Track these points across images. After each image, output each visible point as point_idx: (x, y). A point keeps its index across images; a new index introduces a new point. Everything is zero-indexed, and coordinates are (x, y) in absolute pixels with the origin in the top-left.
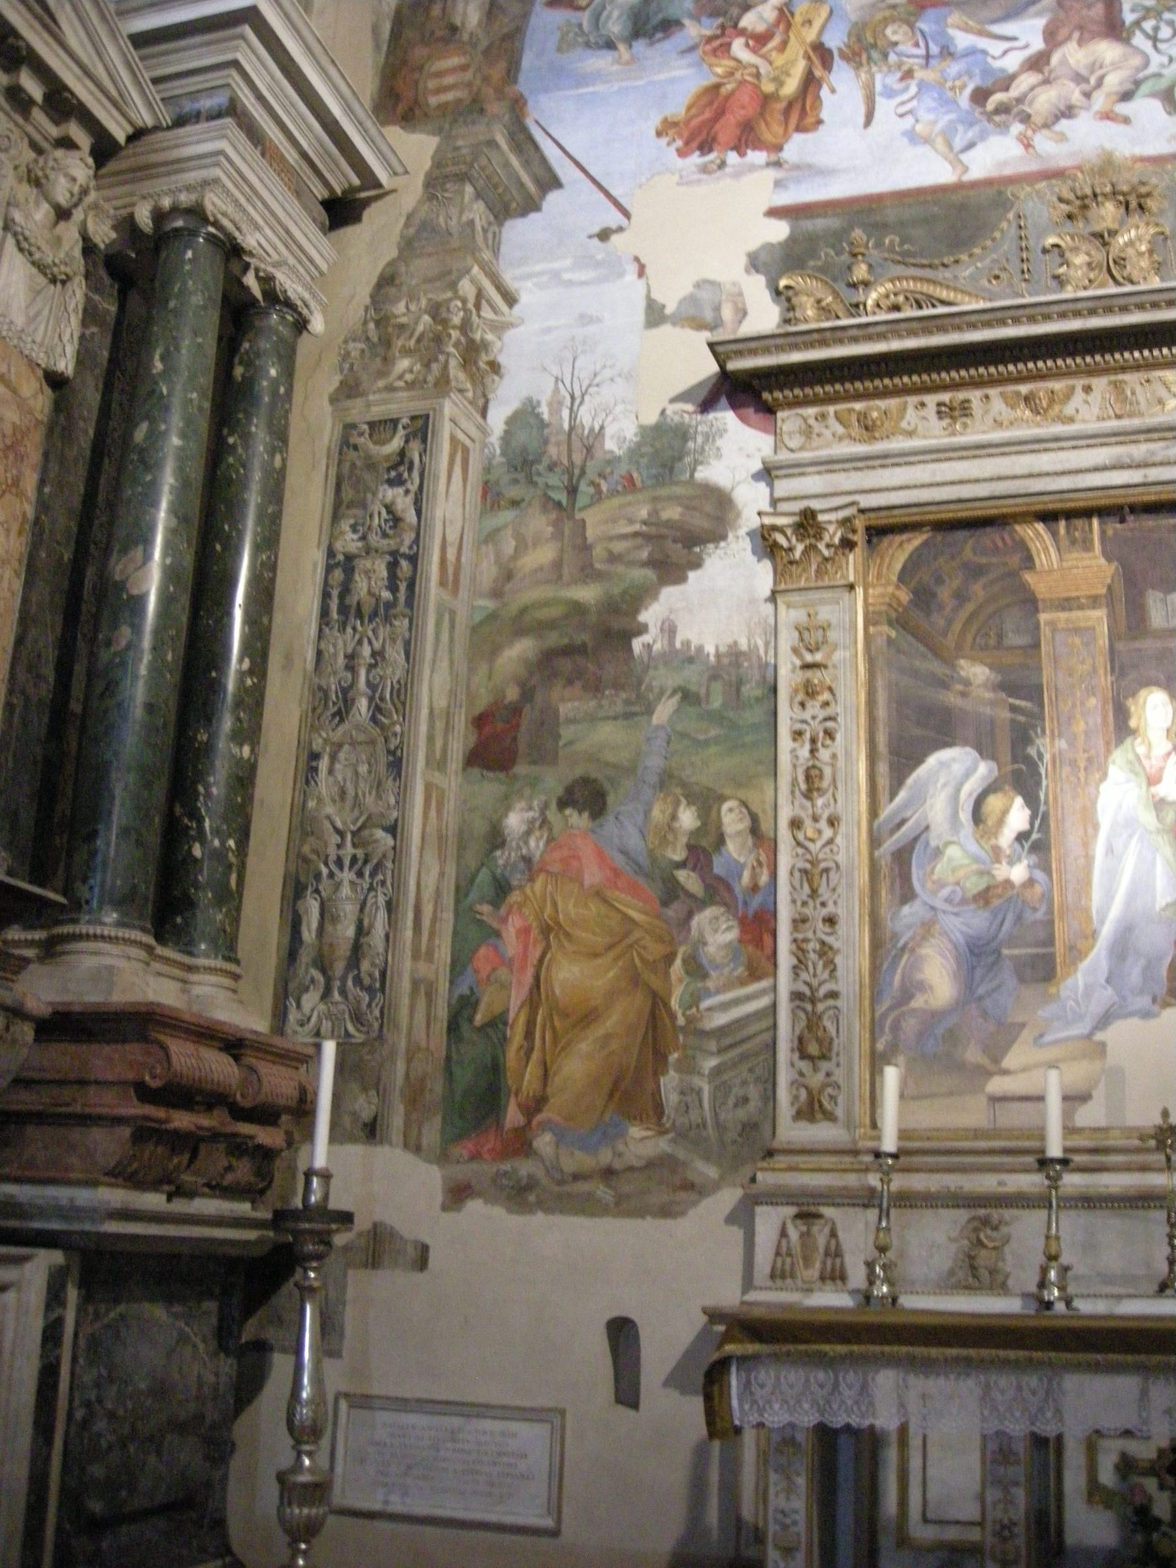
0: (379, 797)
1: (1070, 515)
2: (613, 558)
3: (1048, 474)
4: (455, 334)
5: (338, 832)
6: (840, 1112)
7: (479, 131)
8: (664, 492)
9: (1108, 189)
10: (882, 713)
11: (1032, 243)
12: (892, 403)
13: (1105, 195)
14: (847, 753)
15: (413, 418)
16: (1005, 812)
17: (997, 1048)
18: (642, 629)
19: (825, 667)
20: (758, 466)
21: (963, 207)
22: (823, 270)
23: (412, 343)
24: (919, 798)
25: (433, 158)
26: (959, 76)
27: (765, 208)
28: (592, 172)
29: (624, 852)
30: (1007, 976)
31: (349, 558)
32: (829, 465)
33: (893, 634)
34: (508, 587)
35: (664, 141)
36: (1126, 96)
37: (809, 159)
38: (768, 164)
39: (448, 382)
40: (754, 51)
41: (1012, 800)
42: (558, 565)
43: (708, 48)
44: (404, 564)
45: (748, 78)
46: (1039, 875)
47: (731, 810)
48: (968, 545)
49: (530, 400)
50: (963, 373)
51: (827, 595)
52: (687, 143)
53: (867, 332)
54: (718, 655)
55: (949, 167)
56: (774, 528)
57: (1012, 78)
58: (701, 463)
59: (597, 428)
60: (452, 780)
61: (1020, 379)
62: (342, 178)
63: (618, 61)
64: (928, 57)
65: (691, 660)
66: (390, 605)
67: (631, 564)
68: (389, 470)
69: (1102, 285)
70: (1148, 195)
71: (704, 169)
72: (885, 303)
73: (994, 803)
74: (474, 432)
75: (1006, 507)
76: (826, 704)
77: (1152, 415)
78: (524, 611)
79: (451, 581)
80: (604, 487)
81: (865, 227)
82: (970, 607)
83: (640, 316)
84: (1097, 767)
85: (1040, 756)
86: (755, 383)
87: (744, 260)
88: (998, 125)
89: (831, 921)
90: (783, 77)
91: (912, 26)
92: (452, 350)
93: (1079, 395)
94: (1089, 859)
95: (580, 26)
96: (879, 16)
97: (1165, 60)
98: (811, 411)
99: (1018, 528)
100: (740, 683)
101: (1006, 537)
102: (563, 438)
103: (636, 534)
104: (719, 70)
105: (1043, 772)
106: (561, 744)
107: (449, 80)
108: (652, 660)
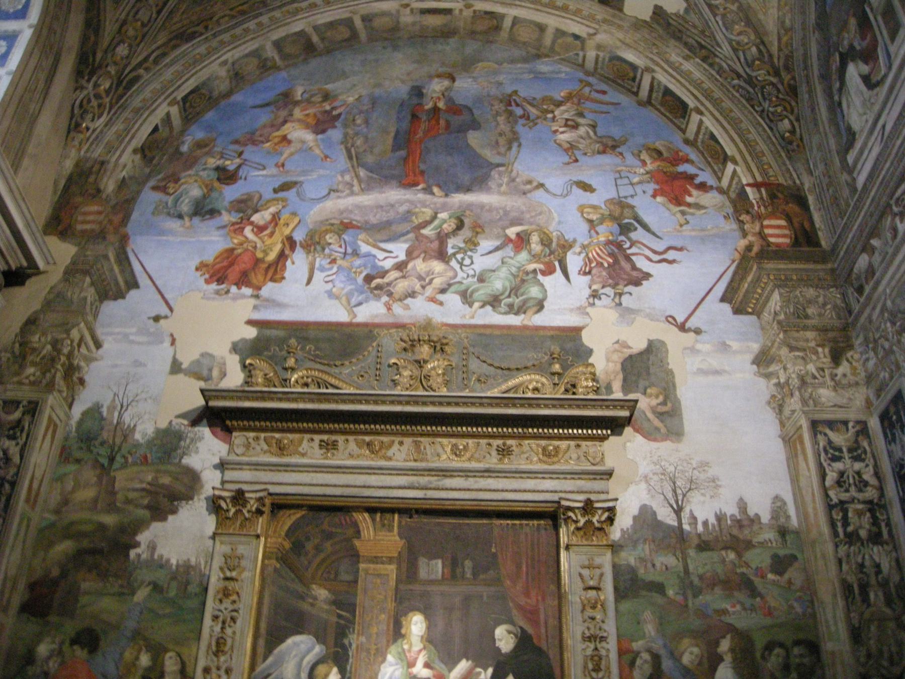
1: (384, 511)
2: (128, 501)
3: (373, 487)
7: (100, 248)
8: (163, 468)
9: (426, 338)
11: (383, 361)
12: (296, 436)
13: (424, 341)
14: (242, 632)
15: (30, 402)
18: (137, 545)
19: (237, 580)
21: (350, 336)
22: (270, 358)
23: (38, 360)
24: (279, 662)
25: (72, 258)
26: (360, 267)
27: (246, 319)
28: (158, 283)
33: (278, 566)
34: (64, 509)
35: (199, 273)
36: (443, 291)
37: (274, 297)
38: (252, 296)
39: (54, 385)
40: (256, 234)
41: (331, 668)
42: (95, 501)
43: (232, 228)
45: (250, 248)
47: (171, 658)
48: (327, 521)
49: (98, 404)
50: (336, 425)
51: (243, 539)
52: (211, 277)
53: (286, 397)
54: (178, 566)
55: (347, 314)
56: (220, 497)
57: (387, 272)
58: (186, 454)
59: (132, 425)
61: (366, 433)
62: (17, 261)
63: (183, 226)
64: (345, 254)
65: (161, 566)
67: (137, 506)
68: (9, 430)
69: (416, 389)
70: (447, 344)
71: (217, 292)
72: (301, 381)
73: (321, 669)
74: (62, 415)
75: (350, 502)
76: (234, 602)
77: (433, 462)
79: (32, 500)
80: (130, 460)
81: (297, 338)
82: (322, 556)
83: (167, 367)
85: (350, 644)
86: (223, 414)
87: (229, 346)
88: (375, 295)
90: (268, 251)
91: (340, 237)
92: (59, 367)
93: (396, 446)
95: (167, 203)
96: (324, 228)
97: (465, 276)
98: (252, 435)
99: (354, 514)
100: (187, 583)
101: (348, 520)
102: (112, 428)
103: (143, 490)
104: (236, 241)
105: (350, 654)
106: (79, 605)
107: (91, 218)
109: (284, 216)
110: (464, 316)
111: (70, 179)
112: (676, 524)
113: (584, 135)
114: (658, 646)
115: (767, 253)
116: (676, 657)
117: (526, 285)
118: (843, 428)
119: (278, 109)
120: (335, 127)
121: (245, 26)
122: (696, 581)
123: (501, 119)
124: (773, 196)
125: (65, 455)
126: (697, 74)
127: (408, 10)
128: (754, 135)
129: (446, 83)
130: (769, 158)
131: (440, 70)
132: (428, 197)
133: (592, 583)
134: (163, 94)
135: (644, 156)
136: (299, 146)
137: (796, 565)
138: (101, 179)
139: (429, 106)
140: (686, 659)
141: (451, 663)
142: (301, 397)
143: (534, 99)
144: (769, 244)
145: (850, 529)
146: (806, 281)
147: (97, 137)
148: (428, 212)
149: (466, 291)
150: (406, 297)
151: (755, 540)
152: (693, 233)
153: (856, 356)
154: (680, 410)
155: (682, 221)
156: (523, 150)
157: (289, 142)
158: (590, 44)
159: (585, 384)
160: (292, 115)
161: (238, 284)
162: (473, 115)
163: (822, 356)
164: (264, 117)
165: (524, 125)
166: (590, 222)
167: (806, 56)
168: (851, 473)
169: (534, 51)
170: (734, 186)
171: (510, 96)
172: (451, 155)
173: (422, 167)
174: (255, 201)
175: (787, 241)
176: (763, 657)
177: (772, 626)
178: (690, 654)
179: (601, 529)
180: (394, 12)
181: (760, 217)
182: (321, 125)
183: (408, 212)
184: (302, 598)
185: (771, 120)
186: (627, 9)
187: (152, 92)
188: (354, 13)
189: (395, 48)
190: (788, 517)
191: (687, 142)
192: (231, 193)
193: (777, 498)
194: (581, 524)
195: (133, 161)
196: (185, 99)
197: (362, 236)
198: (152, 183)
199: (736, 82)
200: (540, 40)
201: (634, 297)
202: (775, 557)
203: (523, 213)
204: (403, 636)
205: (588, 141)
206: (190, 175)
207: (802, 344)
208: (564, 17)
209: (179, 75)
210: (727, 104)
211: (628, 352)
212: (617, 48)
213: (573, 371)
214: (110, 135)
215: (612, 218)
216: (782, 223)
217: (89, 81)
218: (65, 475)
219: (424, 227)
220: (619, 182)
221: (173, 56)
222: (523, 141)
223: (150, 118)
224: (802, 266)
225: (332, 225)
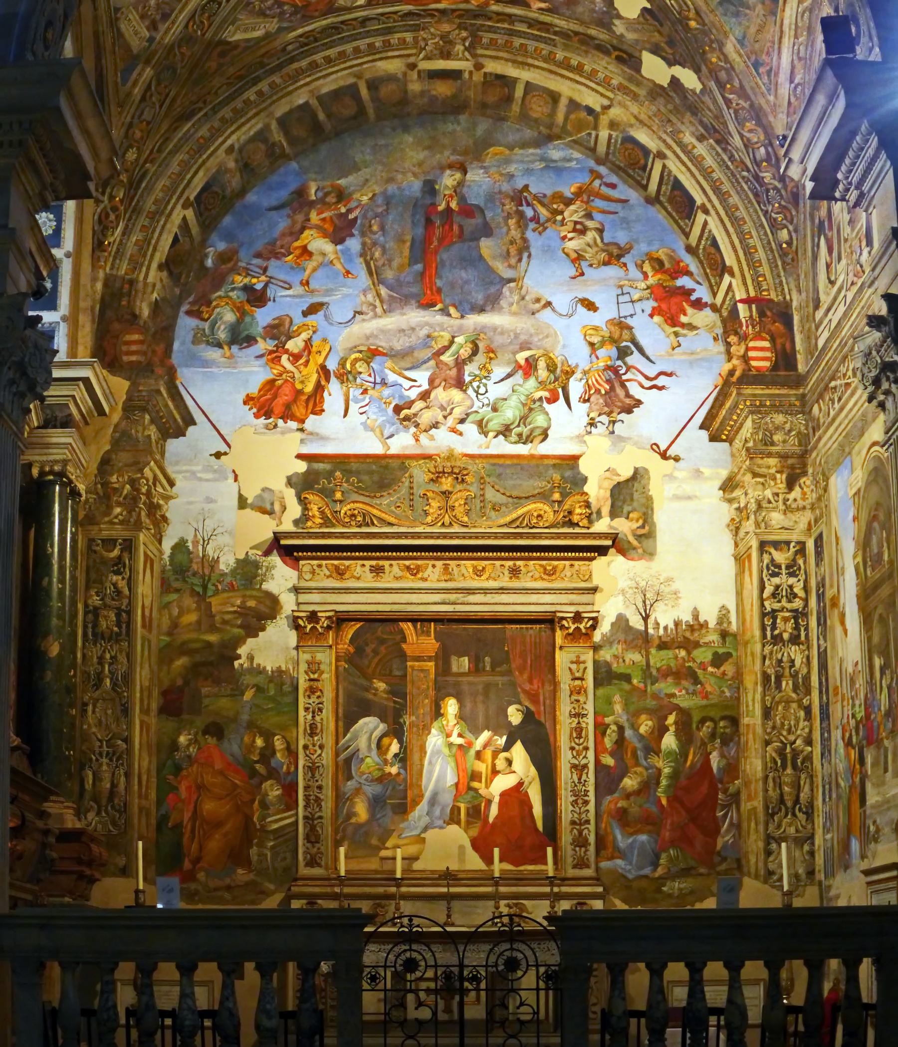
0: (118, 725)
1: (422, 621)
2: (225, 622)
4: (143, 498)
5: (100, 741)
6: (323, 863)
8: (248, 593)
10: (341, 700)
11: (415, 491)
15: (124, 540)
16: (390, 745)
17: (384, 839)
18: (239, 657)
20: (290, 585)
21: (386, 467)
24: (355, 737)
29: (232, 755)
30: (390, 813)
31: (96, 609)
32: (323, 590)
35: (248, 407)
36: (462, 421)
37: (317, 430)
38: (298, 430)
42: (199, 622)
44: (124, 615)
46: (402, 771)
48: (380, 629)
57: (413, 402)
60: (153, 720)
63: (224, 356)
64: (375, 383)
65: (260, 673)
66: (118, 634)
67: (233, 626)
68: (113, 566)
71: (267, 427)
72: (349, 513)
73: (386, 741)
76: (319, 697)
78: (184, 643)
79: (148, 625)
82: (379, 657)
83: (235, 502)
84: (427, 729)
87: (285, 480)
89: (320, 788)
93: (430, 568)
94: (422, 766)
95: (204, 330)
96: (353, 356)
98: (315, 562)
100: (282, 684)
103: (235, 612)
104: (275, 372)
107: (134, 348)
108: (243, 671)
109: (316, 342)
110: (480, 447)
111: (104, 304)
112: (643, 628)
113: (591, 242)
114: (623, 720)
115: (750, 377)
116: (635, 727)
117: (533, 415)
118: (786, 548)
119: (294, 212)
120: (352, 235)
121: (245, 96)
122: (654, 672)
123: (512, 222)
124: (762, 314)
125: (165, 586)
126: (709, 161)
127: (414, 75)
129: (458, 176)
130: (765, 269)
131: (453, 158)
132: (446, 318)
133: (578, 675)
134: (174, 193)
135: (647, 267)
136: (320, 259)
137: (730, 660)
138: (135, 301)
139: (440, 208)
142: (355, 535)
143: (545, 196)
145: (776, 632)
146: (777, 408)
147: (118, 249)
148: (447, 336)
149: (482, 420)
150: (431, 428)
151: (702, 641)
152: (683, 357)
153: (808, 483)
154: (655, 532)
155: (676, 344)
157: (310, 254)
158: (604, 120)
160: (309, 220)
161: (285, 417)
162: (485, 218)
163: (779, 481)
164: (283, 224)
165: (534, 230)
166: (592, 345)
168: (785, 587)
170: (727, 302)
172: (465, 269)
173: (439, 283)
174: (287, 326)
175: (767, 364)
177: (706, 706)
178: (646, 726)
179: (586, 634)
180: (400, 76)
181: (744, 338)
182: (338, 235)
183: (429, 336)
184: (367, 689)
185: (775, 226)
186: (644, 72)
187: (162, 190)
188: (359, 76)
189: (406, 129)
190: (730, 623)
191: (689, 249)
192: (263, 317)
194: (571, 631)
195: (161, 280)
196: (198, 197)
197: (389, 363)
198: (185, 307)
199: (745, 174)
200: (553, 113)
201: (628, 424)
202: (716, 654)
203: (531, 335)
204: (442, 715)
205: (595, 249)
206: (220, 297)
207: (763, 471)
208: (578, 82)
209: (185, 166)
210: (735, 199)
212: (631, 126)
214: (130, 248)
215: (613, 341)
216: (766, 344)
217: (103, 193)
218: (170, 603)
219: (443, 353)
220: (621, 299)
221: (175, 140)
222: (533, 251)
223: (168, 226)
224: (777, 392)
225: (360, 352)
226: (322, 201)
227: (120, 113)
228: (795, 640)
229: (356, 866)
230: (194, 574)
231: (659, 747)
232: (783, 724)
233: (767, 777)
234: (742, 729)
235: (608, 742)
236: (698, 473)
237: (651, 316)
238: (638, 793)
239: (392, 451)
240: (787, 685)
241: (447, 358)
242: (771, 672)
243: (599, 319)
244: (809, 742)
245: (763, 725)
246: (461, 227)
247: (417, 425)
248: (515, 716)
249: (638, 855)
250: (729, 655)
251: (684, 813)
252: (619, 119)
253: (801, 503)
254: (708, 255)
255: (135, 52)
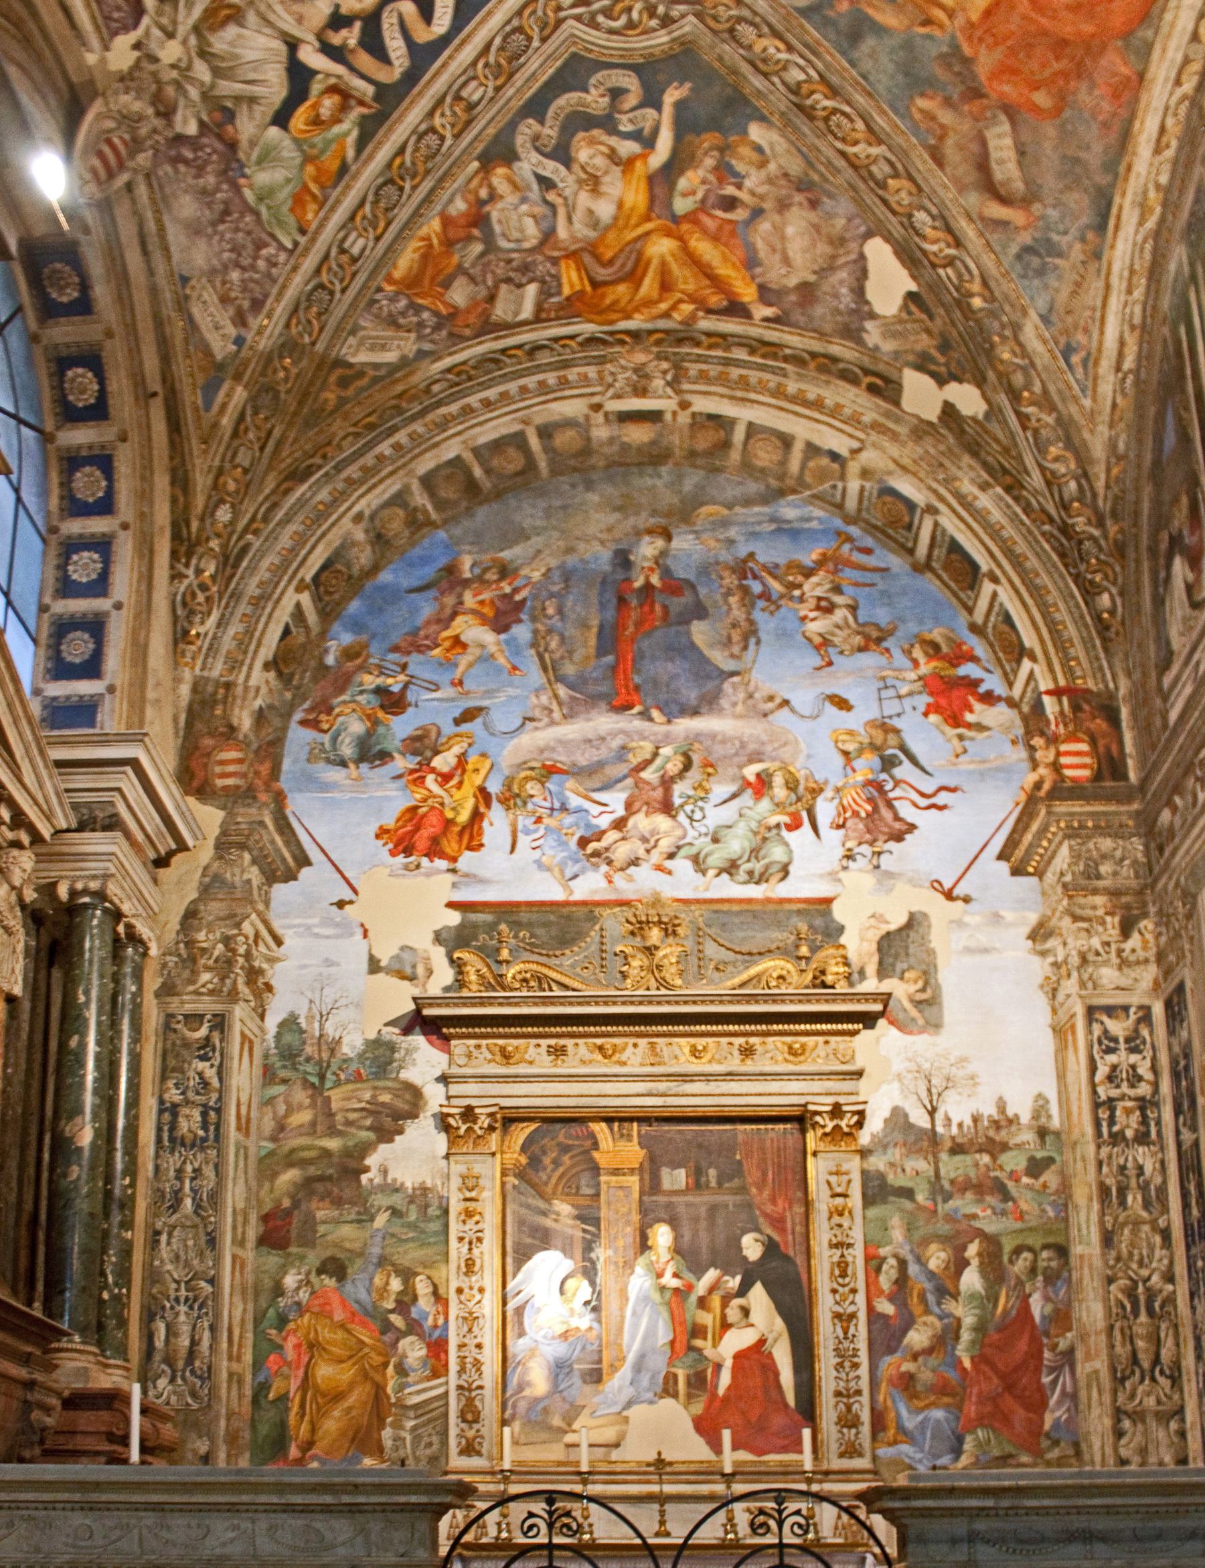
1: (622, 1120)
2: (349, 1123)
8: (381, 1084)
18: (367, 1169)
21: (568, 918)
22: (479, 949)
32: (482, 1078)
36: (671, 856)
42: (313, 1124)
48: (562, 1133)
57: (604, 832)
61: (597, 1035)
65: (397, 1190)
67: (360, 1128)
71: (406, 867)
73: (571, 1284)
83: (364, 966)
84: (629, 1266)
87: (431, 936)
89: (479, 1346)
93: (630, 1049)
96: (523, 774)
98: (472, 1042)
100: (427, 1206)
109: (472, 759)
110: (696, 889)
114: (905, 1252)
115: (1062, 790)
116: (921, 1261)
117: (769, 845)
120: (520, 621)
122: (947, 1186)
123: (733, 600)
124: (1076, 708)
128: (1062, 615)
129: (660, 543)
130: (1078, 650)
131: (652, 521)
132: (647, 724)
133: (839, 1190)
135: (918, 653)
136: (478, 652)
139: (638, 584)
140: (933, 1264)
141: (699, 1272)
143: (777, 566)
144: (1063, 779)
145: (1116, 1129)
148: (647, 748)
151: (1012, 1143)
152: (972, 767)
156: (764, 648)
157: (464, 646)
158: (853, 467)
159: (835, 969)
166: (846, 754)
167: (1138, 502)
168: (1124, 1067)
169: (774, 483)
171: (745, 561)
173: (637, 679)
175: (1086, 773)
176: (1011, 1262)
177: (1022, 1231)
178: (937, 1258)
179: (849, 1134)
181: (1053, 740)
182: (502, 619)
183: (623, 748)
184: (544, 1214)
185: (1090, 591)
190: (1049, 1117)
191: (974, 628)
192: (401, 727)
193: (1040, 1096)
197: (571, 783)
199: (1047, 528)
201: (896, 855)
202: (1032, 1160)
207: (1088, 912)
210: (1033, 562)
211: (886, 928)
212: (890, 473)
213: (821, 955)
215: (874, 747)
220: (884, 694)
222: (763, 636)
224: (1102, 808)
226: (480, 579)
227: (205, 452)
228: (1142, 1138)
229: (530, 1455)
230: (308, 1060)
231: (957, 1287)
232: (1131, 1254)
233: (1111, 1327)
234: (1073, 1261)
235: (885, 1281)
236: (996, 918)
237: (926, 714)
238: (929, 1351)
239: (577, 896)
240: (1134, 1199)
241: (649, 775)
242: (1110, 1182)
243: (856, 720)
244: (1169, 1278)
245: (1103, 1255)
246: (665, 608)
247: (610, 863)
248: (751, 1247)
249: (933, 1438)
250: (1051, 1160)
251: (995, 1380)
252: (873, 465)
253: (1141, 954)
254: (999, 635)
255: (219, 357)
